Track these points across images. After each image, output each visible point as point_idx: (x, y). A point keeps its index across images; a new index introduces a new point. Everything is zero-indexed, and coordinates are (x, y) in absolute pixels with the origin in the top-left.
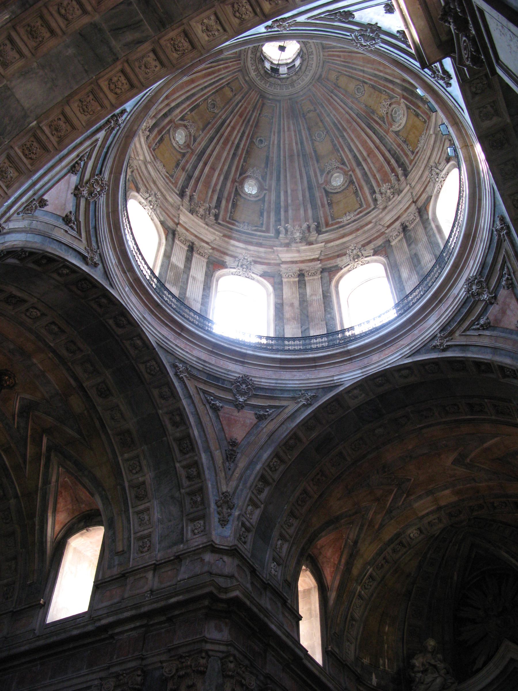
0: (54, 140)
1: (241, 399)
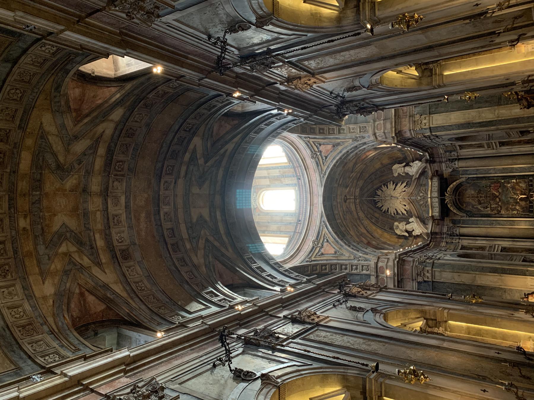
0: (328, 267)
1: (318, 154)
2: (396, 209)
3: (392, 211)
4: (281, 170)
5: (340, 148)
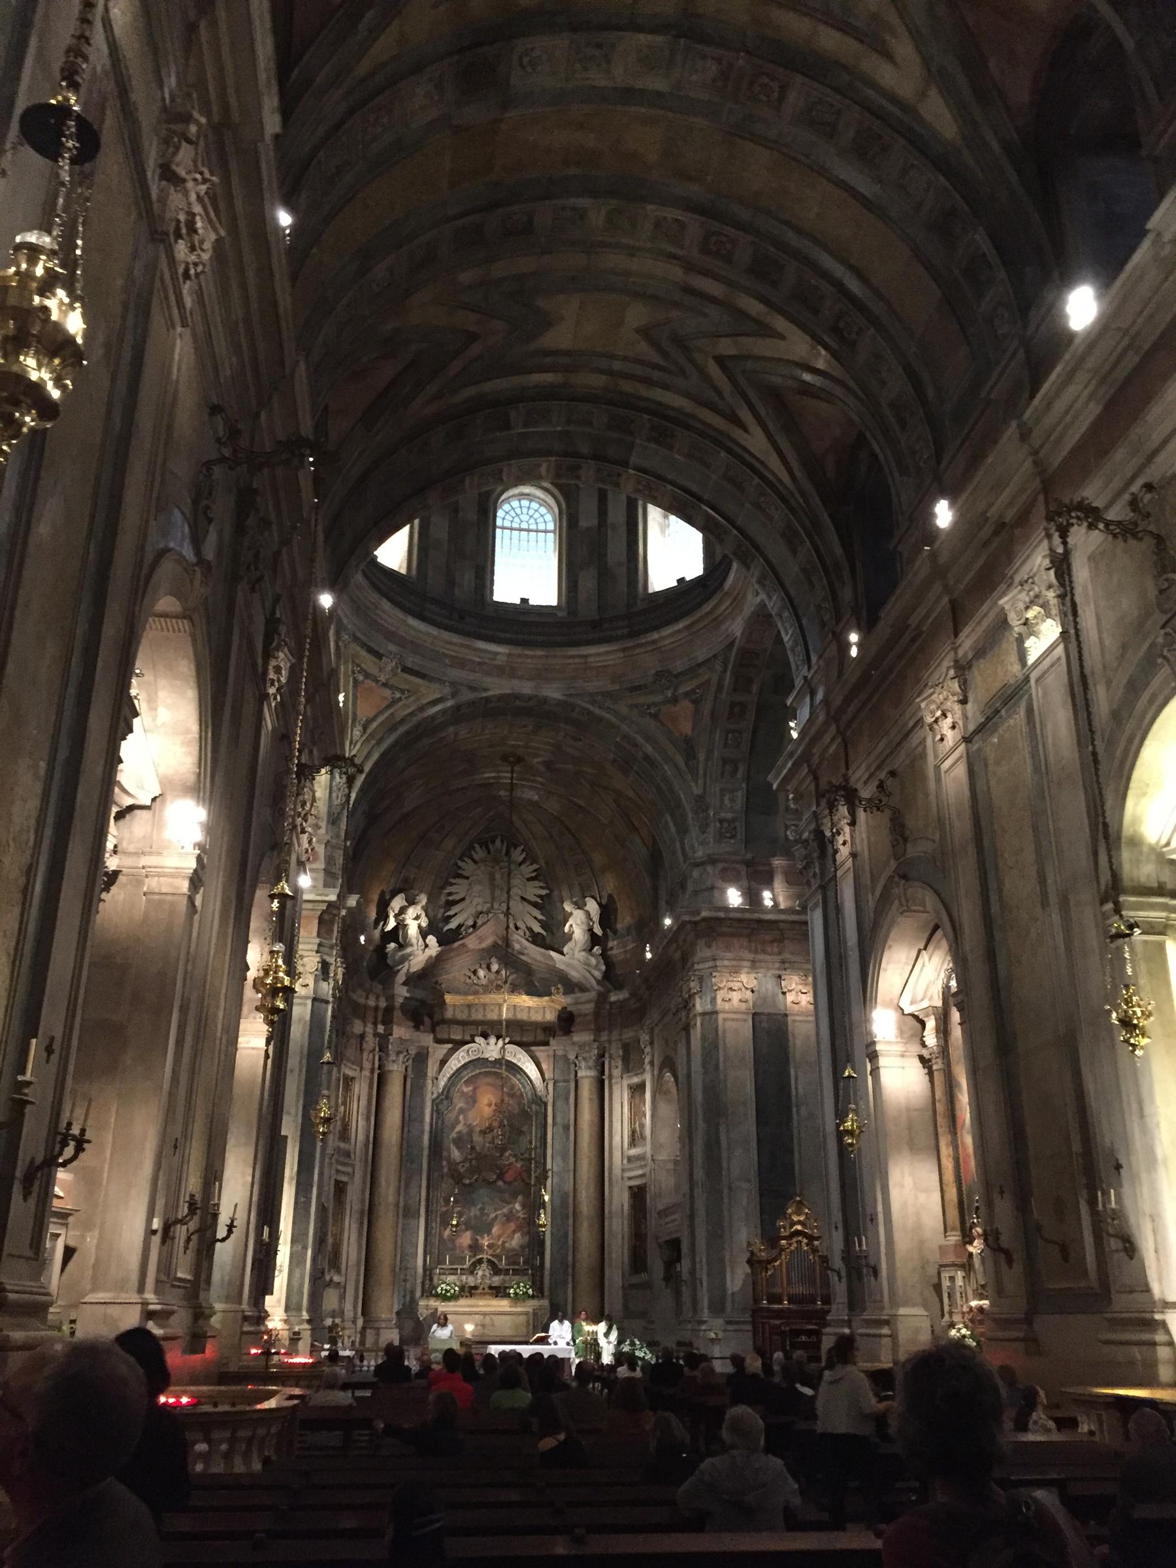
2: (463, 899)
3: (458, 889)
4: (624, 570)
5: (680, 760)
